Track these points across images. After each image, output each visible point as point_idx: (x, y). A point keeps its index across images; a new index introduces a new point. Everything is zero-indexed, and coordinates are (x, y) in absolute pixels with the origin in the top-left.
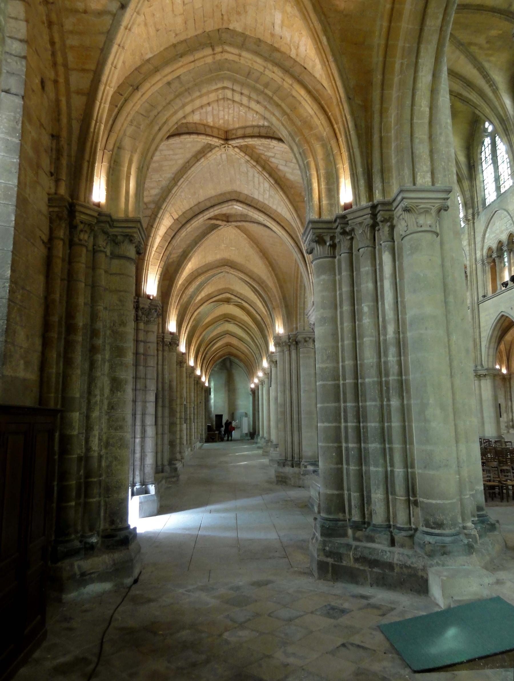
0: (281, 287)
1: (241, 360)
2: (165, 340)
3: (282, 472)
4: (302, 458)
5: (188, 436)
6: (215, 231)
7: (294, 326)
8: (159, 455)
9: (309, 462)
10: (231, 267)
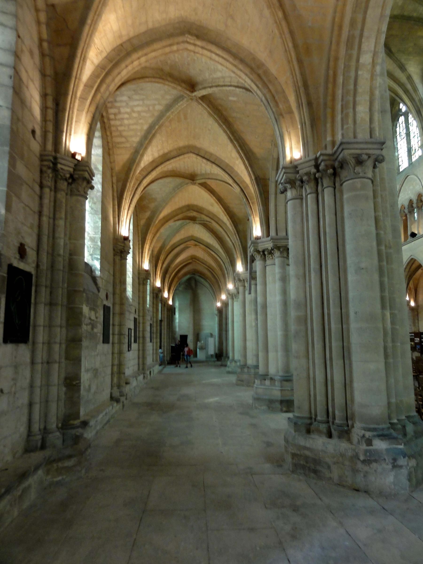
0: (300, 61)
2: (59, 166)
3: (305, 448)
4: (353, 418)
5: (141, 360)
7: (329, 138)
8: (37, 408)
9: (375, 430)
10: (198, 37)
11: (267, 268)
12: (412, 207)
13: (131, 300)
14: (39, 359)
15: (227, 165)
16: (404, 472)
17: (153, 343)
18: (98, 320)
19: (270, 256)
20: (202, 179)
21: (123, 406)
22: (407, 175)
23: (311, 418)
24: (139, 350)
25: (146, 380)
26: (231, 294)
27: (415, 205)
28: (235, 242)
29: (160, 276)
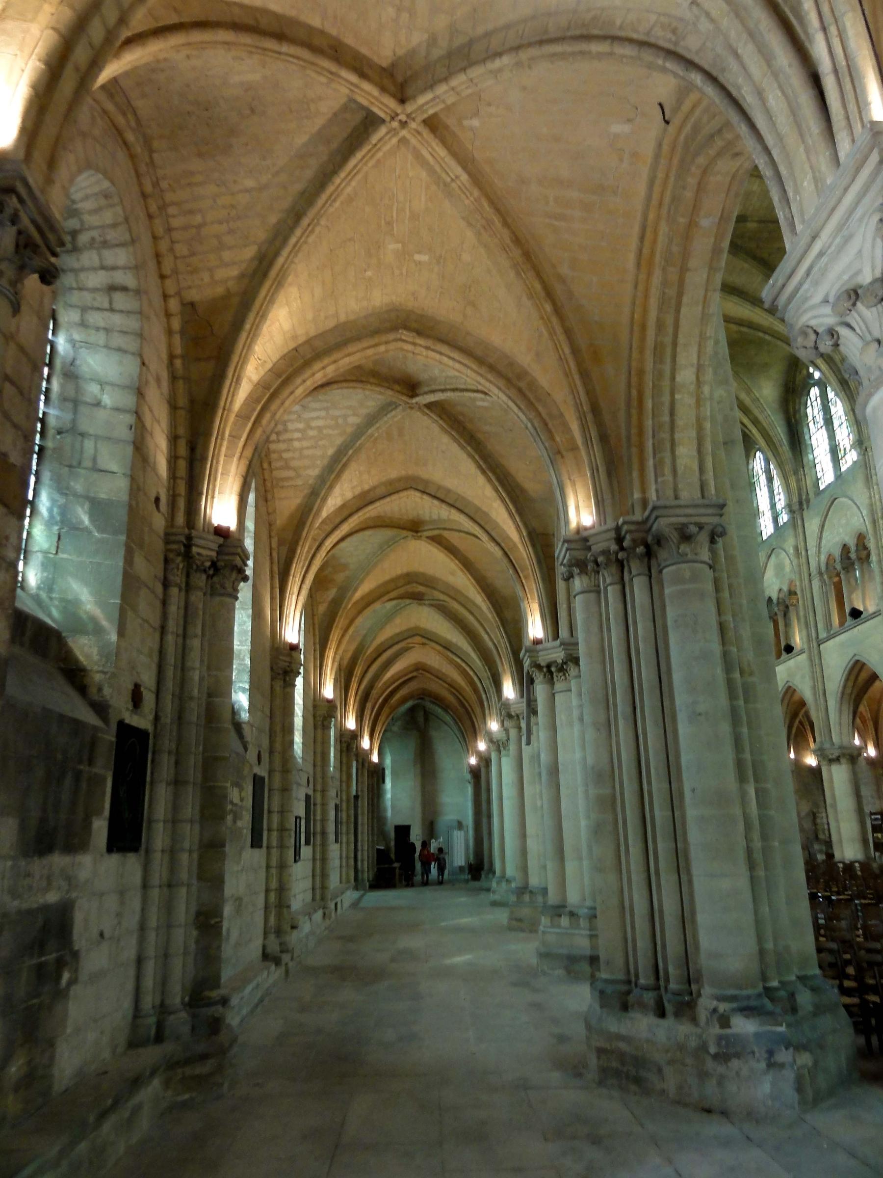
0: (585, 375)
1: (446, 708)
2: (195, 550)
3: (620, 1037)
4: (698, 981)
5: (318, 879)
6: (359, 155)
7: (637, 495)
8: (150, 967)
10: (419, 333)
11: (557, 696)
12: (849, 558)
13: (300, 761)
14: (155, 880)
15: (478, 509)
16: (789, 1075)
17: (341, 843)
18: (244, 803)
19: (561, 674)
20: (434, 529)
21: (287, 972)
22: (832, 498)
23: (629, 982)
24: (314, 859)
25: (328, 922)
26: (495, 740)
27: (853, 556)
28: (499, 642)
29: (355, 708)
